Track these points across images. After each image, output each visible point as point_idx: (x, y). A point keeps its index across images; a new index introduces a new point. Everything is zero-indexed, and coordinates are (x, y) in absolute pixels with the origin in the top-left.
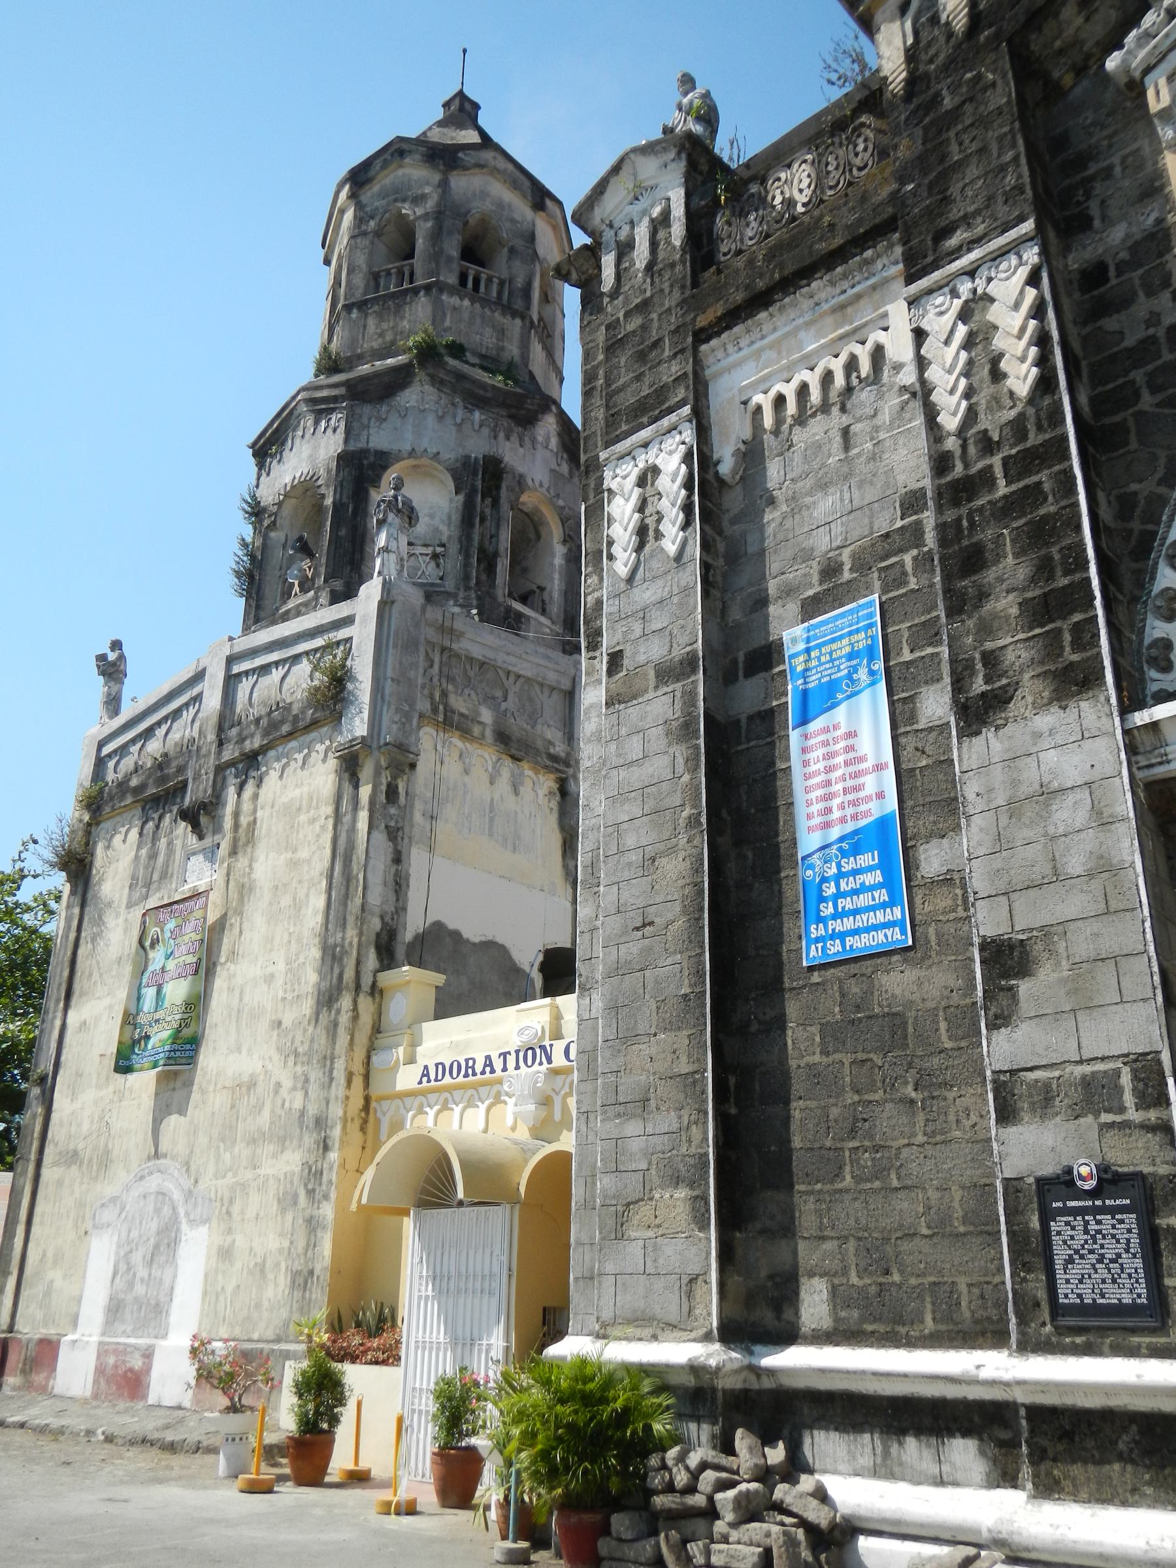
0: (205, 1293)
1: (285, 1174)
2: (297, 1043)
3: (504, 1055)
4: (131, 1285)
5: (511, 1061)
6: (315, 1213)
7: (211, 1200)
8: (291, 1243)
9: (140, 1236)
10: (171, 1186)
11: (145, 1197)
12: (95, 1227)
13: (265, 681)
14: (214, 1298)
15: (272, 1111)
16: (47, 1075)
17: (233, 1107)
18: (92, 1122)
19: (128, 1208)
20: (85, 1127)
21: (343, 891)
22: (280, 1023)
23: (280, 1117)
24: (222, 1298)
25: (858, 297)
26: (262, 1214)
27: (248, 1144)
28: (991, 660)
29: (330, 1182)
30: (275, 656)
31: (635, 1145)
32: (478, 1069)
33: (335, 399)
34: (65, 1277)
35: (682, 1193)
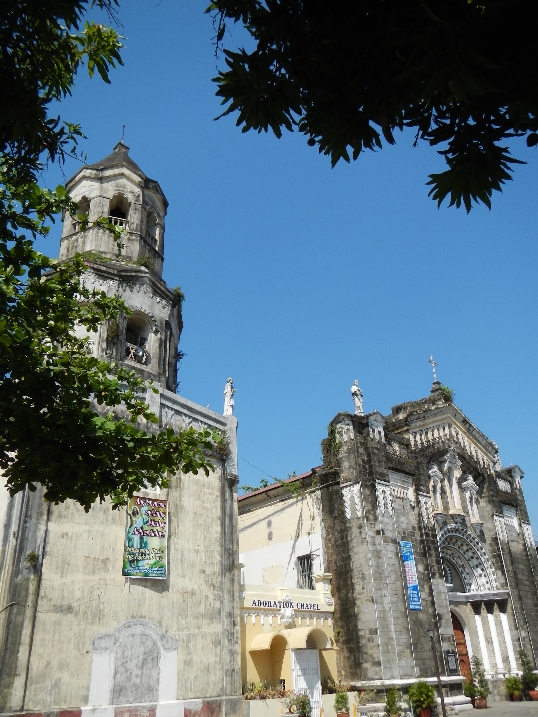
0: (179, 680)
1: (215, 633)
2: (214, 581)
3: (280, 602)
4: (129, 679)
5: (282, 604)
6: (233, 648)
7: (176, 640)
8: (220, 659)
9: (132, 655)
10: (151, 632)
11: (133, 636)
12: (94, 649)
13: (178, 417)
14: (184, 682)
15: (205, 606)
16: (38, 556)
18: (83, 592)
20: (78, 594)
21: (230, 530)
22: (204, 572)
23: (209, 609)
24: (188, 682)
25: (405, 481)
26: (205, 647)
27: (194, 618)
28: (433, 566)
29: (238, 637)
30: (185, 411)
31: (401, 640)
32: (272, 605)
33: (167, 296)
34: (72, 676)
35: (409, 651)
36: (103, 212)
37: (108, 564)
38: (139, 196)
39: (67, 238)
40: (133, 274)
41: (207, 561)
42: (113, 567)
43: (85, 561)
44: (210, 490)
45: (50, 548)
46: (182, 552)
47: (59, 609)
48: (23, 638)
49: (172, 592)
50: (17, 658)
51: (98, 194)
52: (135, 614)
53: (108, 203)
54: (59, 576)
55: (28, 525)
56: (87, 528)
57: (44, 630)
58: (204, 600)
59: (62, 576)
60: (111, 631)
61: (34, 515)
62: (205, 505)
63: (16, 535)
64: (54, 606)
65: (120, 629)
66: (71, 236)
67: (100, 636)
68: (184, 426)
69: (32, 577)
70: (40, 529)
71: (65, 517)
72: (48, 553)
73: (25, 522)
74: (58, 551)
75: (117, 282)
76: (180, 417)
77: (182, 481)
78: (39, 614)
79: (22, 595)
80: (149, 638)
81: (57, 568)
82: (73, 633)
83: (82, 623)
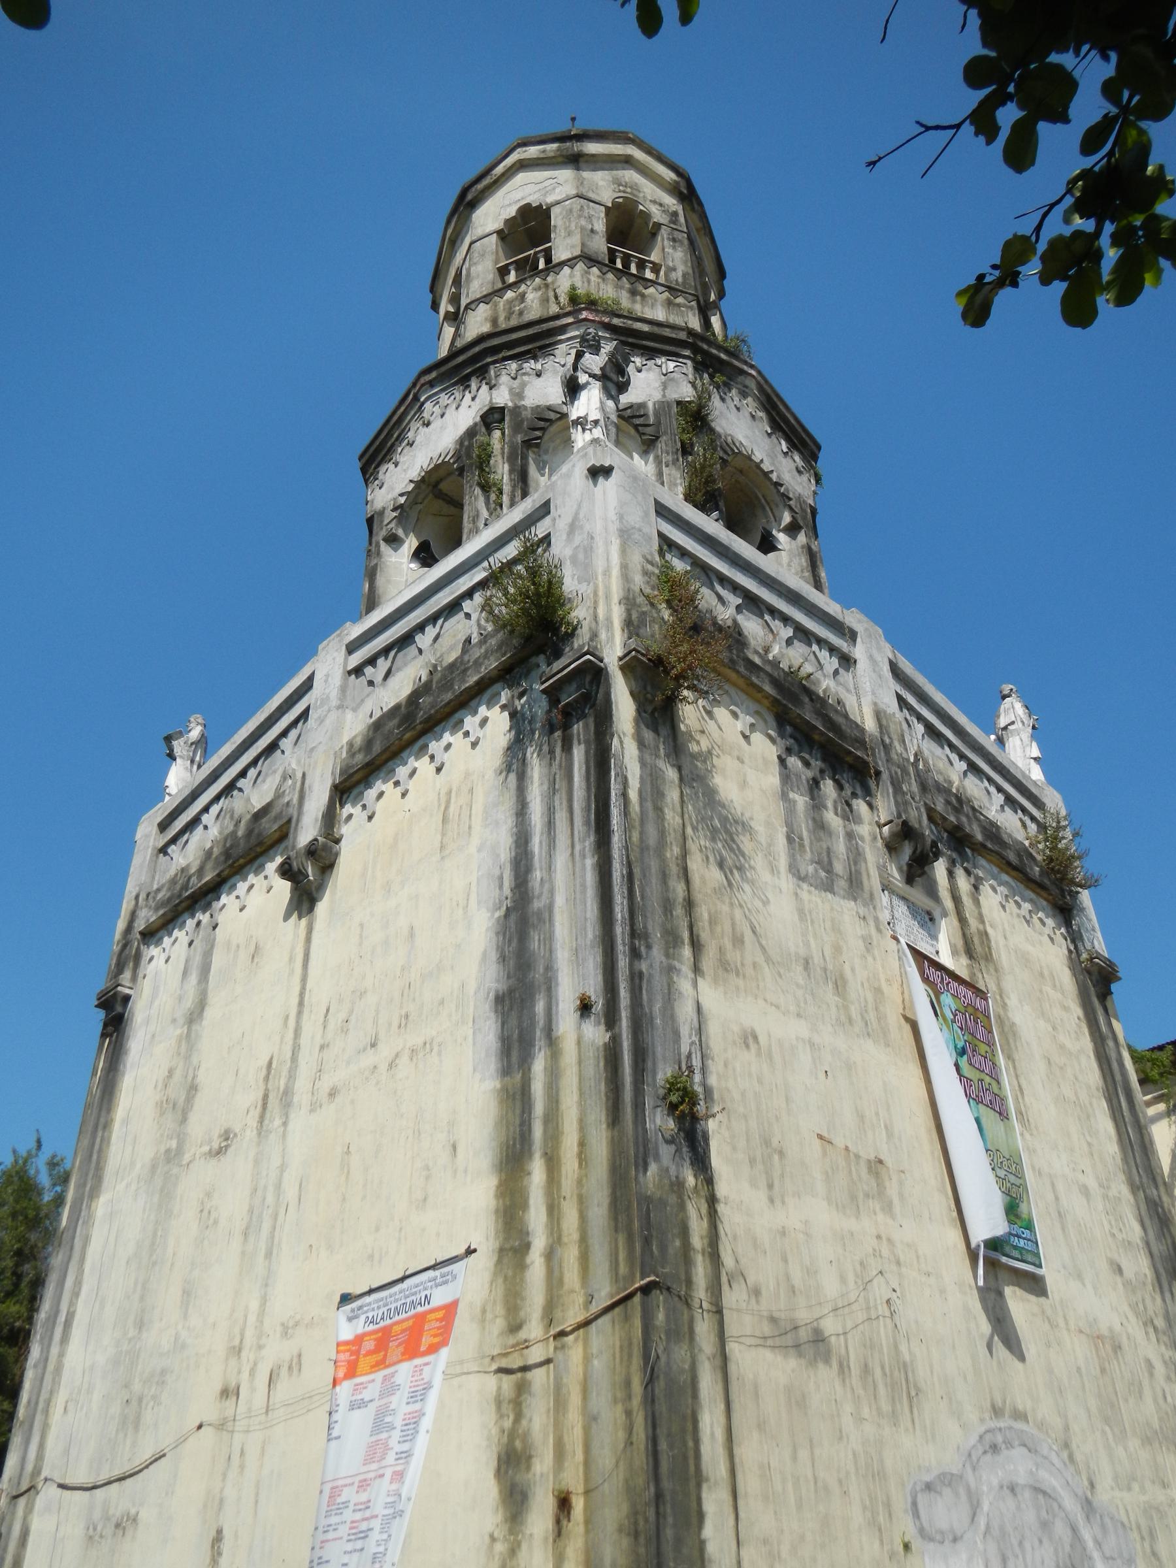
7: (1123, 1524)
10: (1054, 1483)
11: (1012, 1489)
15: (1155, 1400)
17: (1103, 1370)
18: (843, 1280)
19: (986, 1507)
20: (831, 1287)
30: (949, 734)
36: (592, 231)
37: (887, 1184)
38: (675, 214)
39: (485, 299)
40: (723, 356)
41: (1115, 1231)
42: (901, 1196)
43: (825, 1153)
44: (1060, 995)
45: (718, 1074)
46: (1053, 1185)
47: (789, 1340)
48: (706, 1449)
49: (1068, 1330)
50: (702, 1544)
51: (574, 192)
52: (999, 1402)
53: (603, 215)
54: (762, 1195)
55: (644, 966)
56: (801, 1029)
57: (761, 1426)
58: (1146, 1374)
59: (771, 1200)
60: (951, 1462)
61: (656, 935)
62: (1063, 1039)
63: (599, 1006)
64: (773, 1320)
65: (974, 1458)
66: (499, 292)
67: (927, 1478)
68: (955, 778)
69: (691, 1180)
70: (680, 993)
71: (738, 975)
72: (716, 1096)
73: (635, 954)
74: (743, 1094)
75: (689, 362)
76: (940, 749)
77: (993, 943)
78: (732, 1347)
79: (671, 1251)
80: (1055, 1505)
81: (752, 1162)
82: (851, 1456)
83: (866, 1412)
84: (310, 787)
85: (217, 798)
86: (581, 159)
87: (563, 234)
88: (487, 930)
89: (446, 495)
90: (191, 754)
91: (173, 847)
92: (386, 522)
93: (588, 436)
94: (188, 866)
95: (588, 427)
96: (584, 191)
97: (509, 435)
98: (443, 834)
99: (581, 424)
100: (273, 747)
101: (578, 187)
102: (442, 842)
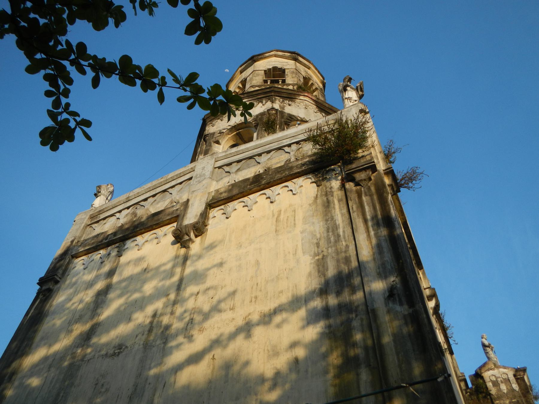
36: (300, 80)
51: (295, 68)
84: (192, 204)
85: (128, 208)
86: (297, 61)
87: (290, 77)
88: (311, 263)
89: (241, 135)
90: (108, 196)
91: (96, 225)
92: (215, 137)
93: (352, 104)
94: (107, 231)
95: (352, 101)
96: (298, 69)
97: (279, 118)
98: (276, 226)
99: (350, 99)
100: (165, 191)
101: (295, 67)
102: (276, 229)
